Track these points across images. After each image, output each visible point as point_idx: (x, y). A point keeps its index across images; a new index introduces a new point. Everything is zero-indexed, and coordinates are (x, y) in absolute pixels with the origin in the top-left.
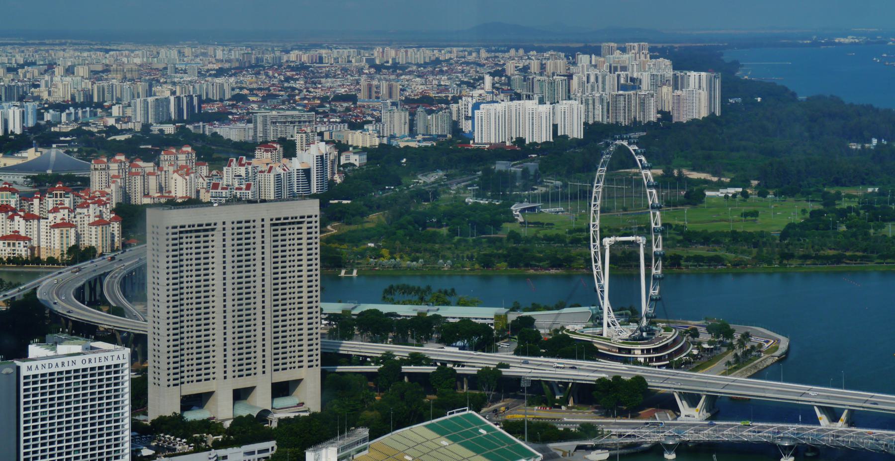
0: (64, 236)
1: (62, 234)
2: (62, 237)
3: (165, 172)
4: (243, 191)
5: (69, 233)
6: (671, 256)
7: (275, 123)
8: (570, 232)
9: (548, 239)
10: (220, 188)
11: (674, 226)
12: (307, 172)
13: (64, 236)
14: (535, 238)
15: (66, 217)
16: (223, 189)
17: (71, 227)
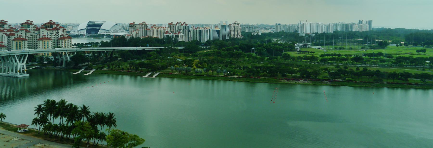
0: (18, 45)
1: (17, 44)
2: (17, 46)
4: (177, 35)
5: (21, 44)
6: (401, 73)
8: (322, 56)
9: (306, 58)
10: (168, 33)
11: (384, 54)
12: (218, 32)
13: (18, 45)
14: (299, 58)
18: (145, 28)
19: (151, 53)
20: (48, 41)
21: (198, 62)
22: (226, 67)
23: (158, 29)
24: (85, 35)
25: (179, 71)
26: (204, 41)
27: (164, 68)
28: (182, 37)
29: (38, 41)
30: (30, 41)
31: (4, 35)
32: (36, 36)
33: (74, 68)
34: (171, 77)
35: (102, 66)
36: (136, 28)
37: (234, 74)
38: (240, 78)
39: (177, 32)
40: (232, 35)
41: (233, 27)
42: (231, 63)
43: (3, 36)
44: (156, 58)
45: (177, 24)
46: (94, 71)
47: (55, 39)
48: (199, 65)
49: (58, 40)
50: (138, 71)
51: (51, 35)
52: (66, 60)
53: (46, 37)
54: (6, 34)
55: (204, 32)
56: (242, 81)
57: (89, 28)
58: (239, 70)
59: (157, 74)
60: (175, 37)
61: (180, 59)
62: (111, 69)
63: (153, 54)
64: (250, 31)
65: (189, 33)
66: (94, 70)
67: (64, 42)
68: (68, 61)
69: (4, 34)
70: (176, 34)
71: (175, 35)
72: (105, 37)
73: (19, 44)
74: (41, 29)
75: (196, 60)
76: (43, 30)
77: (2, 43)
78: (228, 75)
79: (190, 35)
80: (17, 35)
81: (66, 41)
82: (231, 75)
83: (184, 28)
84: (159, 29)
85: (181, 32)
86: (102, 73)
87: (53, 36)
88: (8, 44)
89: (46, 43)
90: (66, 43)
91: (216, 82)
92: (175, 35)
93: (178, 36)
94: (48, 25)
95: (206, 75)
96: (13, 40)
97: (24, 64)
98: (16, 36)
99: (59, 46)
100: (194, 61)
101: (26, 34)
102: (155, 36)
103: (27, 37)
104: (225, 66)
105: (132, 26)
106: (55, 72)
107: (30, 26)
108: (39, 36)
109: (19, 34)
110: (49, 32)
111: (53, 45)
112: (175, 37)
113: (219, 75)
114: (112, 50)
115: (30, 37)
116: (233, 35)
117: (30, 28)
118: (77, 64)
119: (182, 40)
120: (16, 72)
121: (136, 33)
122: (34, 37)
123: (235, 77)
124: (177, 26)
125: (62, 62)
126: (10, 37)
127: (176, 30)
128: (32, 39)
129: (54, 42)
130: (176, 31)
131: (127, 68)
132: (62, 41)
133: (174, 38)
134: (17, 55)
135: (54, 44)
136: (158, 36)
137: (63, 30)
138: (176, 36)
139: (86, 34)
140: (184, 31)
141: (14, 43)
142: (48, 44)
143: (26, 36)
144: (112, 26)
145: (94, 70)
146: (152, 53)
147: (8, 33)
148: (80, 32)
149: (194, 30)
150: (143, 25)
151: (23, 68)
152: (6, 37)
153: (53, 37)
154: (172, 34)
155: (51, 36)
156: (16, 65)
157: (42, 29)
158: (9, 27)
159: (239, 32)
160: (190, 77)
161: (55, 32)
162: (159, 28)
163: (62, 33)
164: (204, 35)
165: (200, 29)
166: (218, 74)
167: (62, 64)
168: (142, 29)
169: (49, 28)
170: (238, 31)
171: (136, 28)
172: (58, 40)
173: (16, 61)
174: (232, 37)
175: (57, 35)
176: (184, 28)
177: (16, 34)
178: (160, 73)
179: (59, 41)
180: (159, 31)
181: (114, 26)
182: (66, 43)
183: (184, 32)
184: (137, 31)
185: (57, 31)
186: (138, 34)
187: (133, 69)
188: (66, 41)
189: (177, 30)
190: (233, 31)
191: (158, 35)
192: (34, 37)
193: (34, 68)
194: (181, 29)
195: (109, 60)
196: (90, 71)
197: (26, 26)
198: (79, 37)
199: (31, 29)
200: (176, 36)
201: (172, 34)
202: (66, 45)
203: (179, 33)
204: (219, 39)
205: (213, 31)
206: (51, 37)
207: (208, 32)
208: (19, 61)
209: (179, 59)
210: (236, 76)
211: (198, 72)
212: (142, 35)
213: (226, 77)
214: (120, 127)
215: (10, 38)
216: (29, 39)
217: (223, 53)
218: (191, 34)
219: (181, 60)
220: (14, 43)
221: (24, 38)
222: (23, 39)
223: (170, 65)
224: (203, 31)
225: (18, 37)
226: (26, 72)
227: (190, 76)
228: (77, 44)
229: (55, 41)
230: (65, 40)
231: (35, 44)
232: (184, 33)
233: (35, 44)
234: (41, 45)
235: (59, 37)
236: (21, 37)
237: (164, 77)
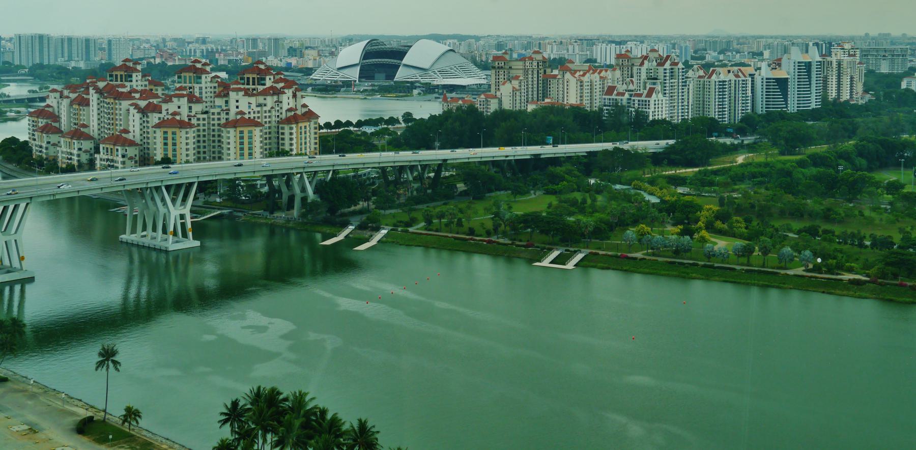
0: (170, 142)
1: (165, 138)
2: (166, 144)
4: (643, 98)
5: (177, 136)
7: (865, 55)
10: (615, 92)
12: (782, 84)
13: (170, 142)
15: (184, 112)
16: (619, 94)
17: (181, 128)
18: (542, 71)
19: (559, 170)
20: (250, 128)
21: (713, 212)
22: (811, 234)
23: (582, 78)
24: (355, 85)
25: (652, 249)
26: (735, 117)
27: (600, 232)
28: (660, 106)
29: (222, 129)
30: (201, 128)
31: (132, 108)
32: (219, 114)
33: (327, 222)
34: (625, 268)
35: (406, 218)
36: (513, 73)
37: (840, 268)
38: (861, 285)
39: (645, 88)
40: (832, 94)
41: (835, 65)
42: (827, 216)
43: (128, 110)
44: (575, 186)
45: (646, 62)
46: (385, 236)
47: (270, 122)
48: (719, 224)
49: (280, 126)
50: (521, 241)
51: (259, 109)
52: (303, 195)
53: (247, 116)
54: (136, 106)
55: (735, 88)
56: (867, 295)
57: (367, 61)
58: (856, 249)
59: (579, 257)
60: (639, 105)
61: (654, 195)
62: (437, 231)
63: (567, 174)
64: (896, 67)
65: (686, 90)
66: (384, 232)
67: (297, 132)
68: (309, 201)
69: (131, 105)
70: (640, 95)
71: (637, 99)
72: (415, 92)
73: (173, 139)
74: (231, 93)
75: (708, 207)
76: (237, 95)
77: (128, 132)
78: (818, 268)
79: (688, 96)
80: (167, 110)
81: (303, 128)
82: (830, 271)
83: (668, 75)
84: (586, 79)
85: (658, 87)
86: (407, 245)
87: (265, 112)
88: (141, 135)
89: (246, 135)
90: (303, 146)
91: (774, 293)
92: (639, 101)
93: (646, 104)
94: (251, 76)
95: (742, 264)
96: (158, 126)
97: (187, 211)
98: (164, 113)
99: (282, 147)
100: (700, 208)
101: (190, 108)
102: (572, 99)
103: (192, 118)
104: (805, 231)
105: (498, 67)
106: (273, 229)
107: (200, 78)
108: (227, 114)
109: (172, 107)
110: (253, 100)
111: (266, 139)
112: (636, 105)
113: (786, 268)
114: (440, 162)
115: (201, 116)
116: (834, 91)
117: (201, 83)
118: (332, 210)
119: (660, 117)
120: (165, 231)
121: (514, 88)
122: (212, 117)
123: (841, 280)
124: (644, 69)
125: (291, 199)
126: (149, 114)
127: (642, 81)
128: (206, 122)
129: (268, 131)
130: (642, 85)
131: (484, 228)
132: (291, 128)
133: (633, 110)
134: (168, 188)
135: (268, 136)
136: (581, 100)
137: (293, 92)
138: (641, 103)
139: (359, 81)
140: (667, 85)
141: (159, 133)
142: (250, 138)
143: (190, 114)
144: (437, 57)
145: (384, 232)
146: (563, 169)
147: (143, 104)
148: (342, 73)
149: (702, 80)
150: (535, 64)
151: (183, 225)
152: (138, 116)
153: (266, 117)
154: (627, 96)
155: (258, 112)
156: (165, 214)
157: (235, 93)
158: (145, 81)
159: (856, 79)
160: (688, 274)
161: (270, 101)
162: (584, 75)
163: (292, 105)
164: (735, 97)
165: (722, 77)
166: (783, 264)
167: (290, 205)
168: (530, 76)
169: (254, 84)
170: (852, 78)
171: (511, 71)
172: (280, 126)
174: (830, 97)
175: (277, 108)
176: (668, 75)
177: (164, 107)
178: (589, 251)
179: (283, 128)
180: (585, 84)
181: (443, 54)
182: (303, 135)
183: (667, 88)
184: (515, 83)
185: (275, 98)
186: (518, 93)
187: (505, 234)
188: (303, 128)
189: (645, 83)
190: (834, 77)
191: (581, 97)
192: (212, 117)
193: (212, 215)
194: (656, 79)
195: (429, 191)
196: (371, 236)
197: (190, 77)
198: (339, 91)
199: (204, 88)
200: (641, 103)
201: (627, 96)
202: (303, 141)
203: (649, 94)
204: (786, 107)
205: (765, 81)
206: (259, 118)
207: (749, 85)
208: (174, 201)
209: (651, 194)
210: (847, 276)
211: (714, 255)
212: (530, 93)
213: (811, 277)
215: (148, 120)
216: (199, 122)
217: (801, 176)
218: (691, 91)
219: (658, 201)
220: (159, 133)
221: (186, 120)
222: (182, 125)
223: (622, 223)
224: (733, 82)
225: (170, 117)
226: (190, 234)
227: (687, 267)
228: (333, 124)
229: (270, 128)
230: (300, 125)
231: (216, 139)
232: (667, 92)
233: (216, 139)
234: (232, 141)
235: (284, 116)
236: (178, 118)
237: (603, 268)
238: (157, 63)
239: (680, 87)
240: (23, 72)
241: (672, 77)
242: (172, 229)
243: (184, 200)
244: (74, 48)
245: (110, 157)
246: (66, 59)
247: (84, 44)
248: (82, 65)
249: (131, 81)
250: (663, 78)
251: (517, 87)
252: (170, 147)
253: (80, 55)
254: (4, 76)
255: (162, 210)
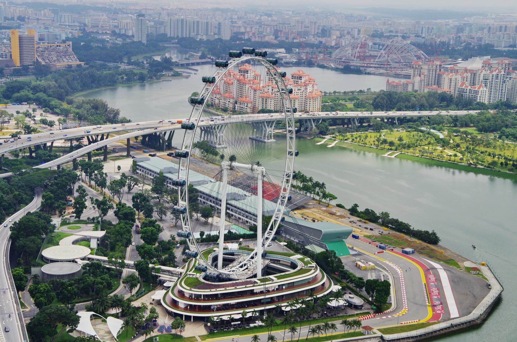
0: (264, 102)
2: (263, 103)
3: (474, 74)
4: (476, 89)
5: (267, 100)
10: (464, 85)
13: (264, 102)
51: (298, 91)
54: (251, 87)
101: (272, 90)
112: (473, 93)
134: (266, 122)
142: (294, 103)
173: (265, 127)
182: (315, 104)
194: (487, 79)
203: (479, 88)
208: (268, 126)
214: (328, 191)
226: (273, 137)
238: (246, 38)
239: (501, 84)
240: (174, 42)
241: (497, 78)
242: (267, 135)
243: (271, 127)
244: (200, 27)
245: (241, 106)
246: (196, 34)
247: (205, 25)
248: (205, 38)
249: (248, 73)
250: (491, 79)
251: (423, 78)
252: (264, 104)
253: (203, 31)
254: (166, 44)
255: (264, 129)
